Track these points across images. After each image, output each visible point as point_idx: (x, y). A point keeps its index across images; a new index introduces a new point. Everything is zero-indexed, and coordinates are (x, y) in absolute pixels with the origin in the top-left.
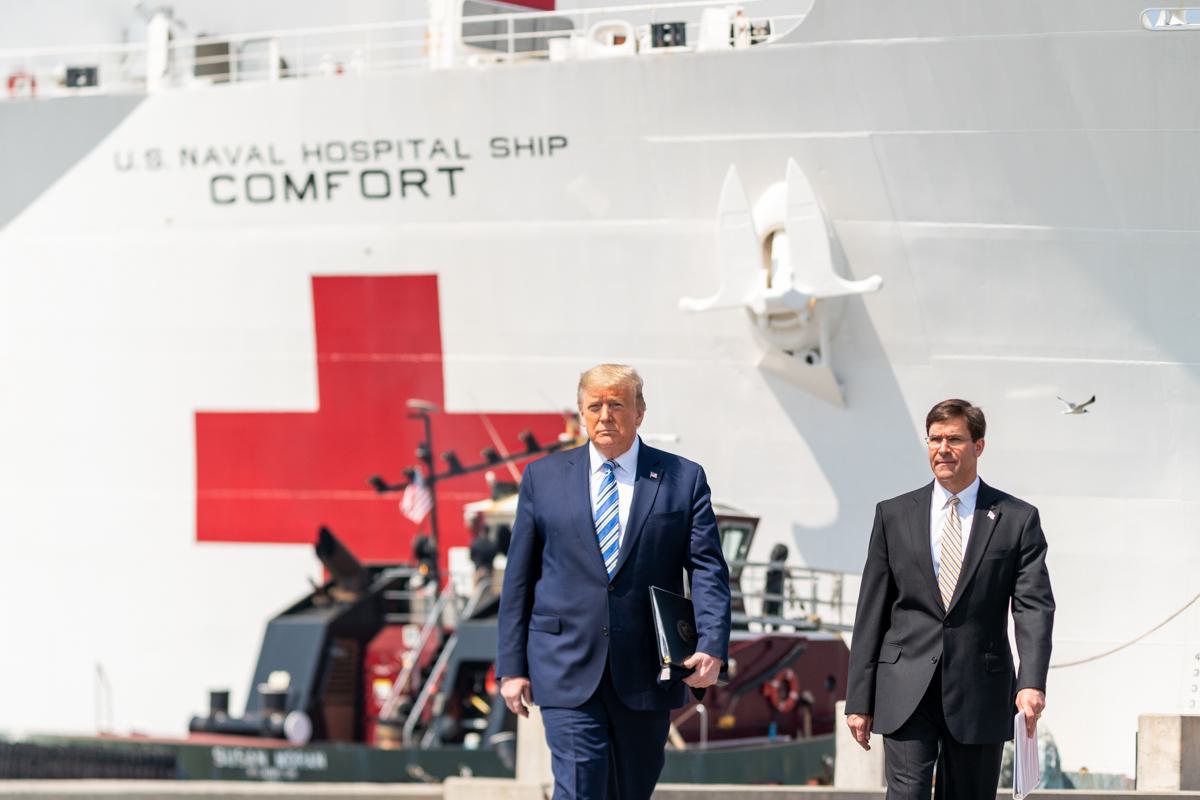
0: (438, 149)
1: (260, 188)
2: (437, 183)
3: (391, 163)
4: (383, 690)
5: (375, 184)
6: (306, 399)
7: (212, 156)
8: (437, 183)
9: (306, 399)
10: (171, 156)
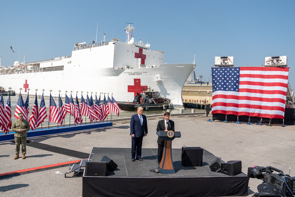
0: (141, 72)
1: (131, 74)
2: (140, 74)
3: (138, 73)
4: (141, 101)
5: (137, 74)
6: (134, 85)
7: (129, 73)
8: (140, 74)
9: (134, 85)
10: (127, 73)
